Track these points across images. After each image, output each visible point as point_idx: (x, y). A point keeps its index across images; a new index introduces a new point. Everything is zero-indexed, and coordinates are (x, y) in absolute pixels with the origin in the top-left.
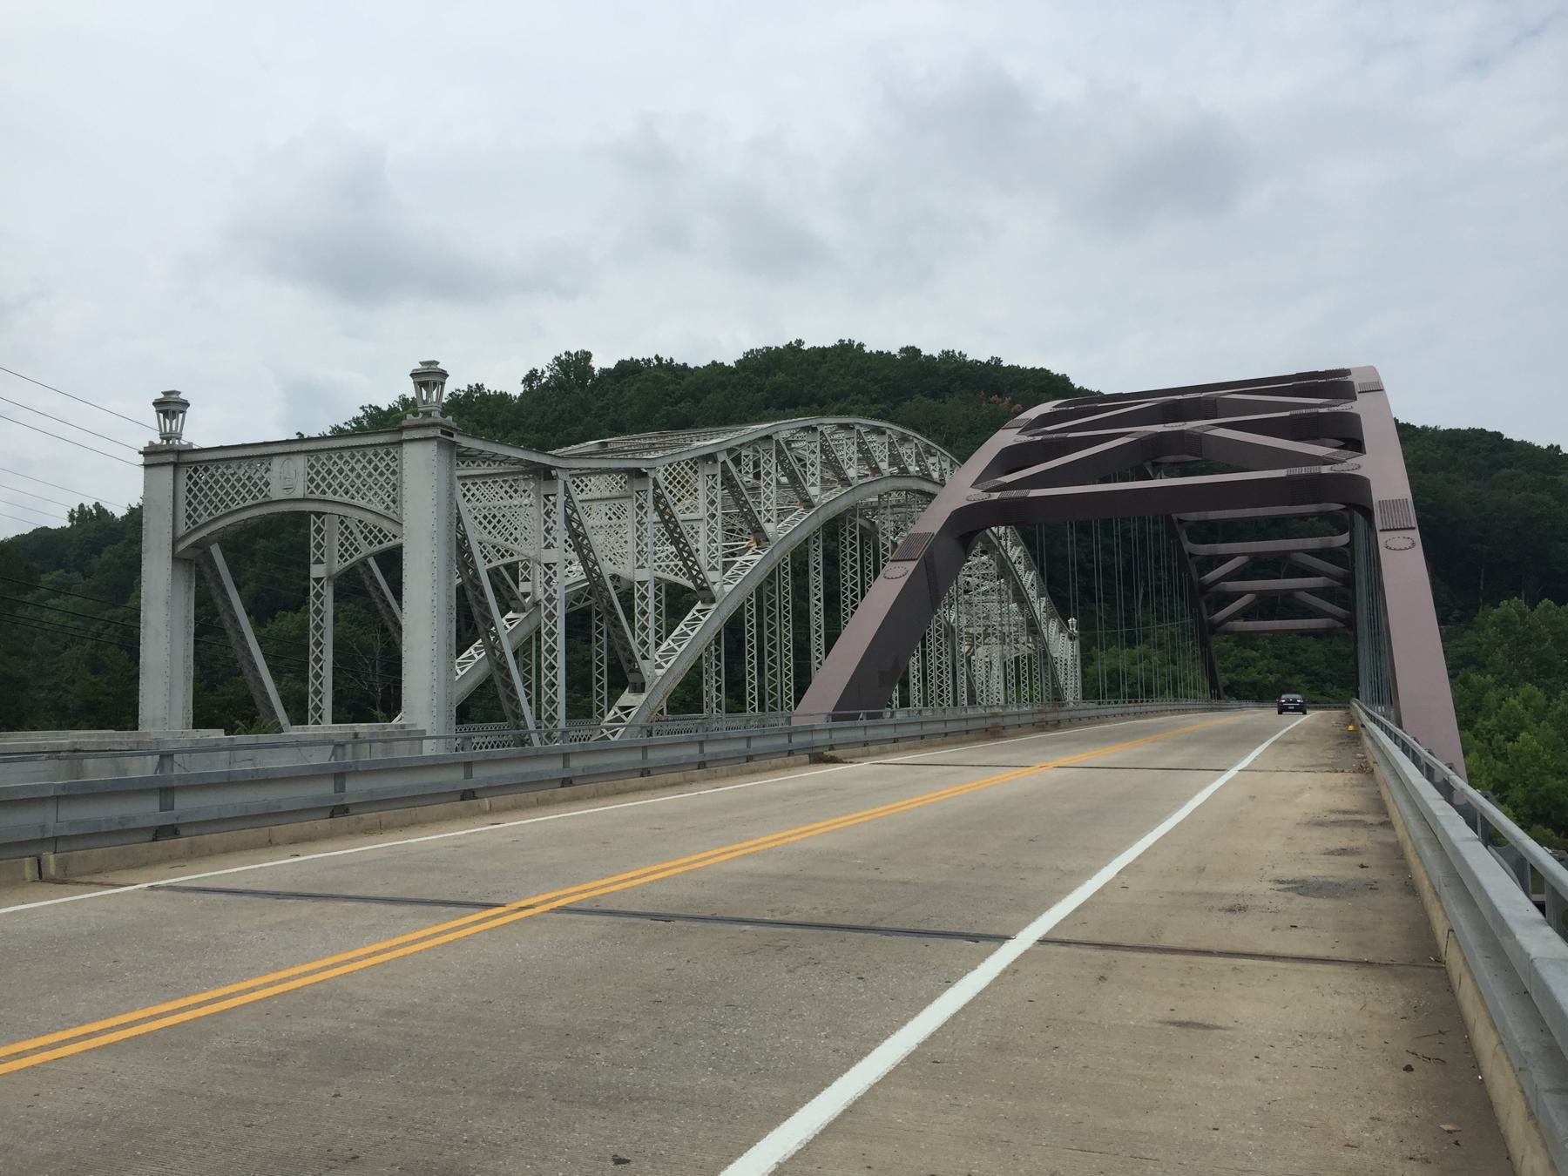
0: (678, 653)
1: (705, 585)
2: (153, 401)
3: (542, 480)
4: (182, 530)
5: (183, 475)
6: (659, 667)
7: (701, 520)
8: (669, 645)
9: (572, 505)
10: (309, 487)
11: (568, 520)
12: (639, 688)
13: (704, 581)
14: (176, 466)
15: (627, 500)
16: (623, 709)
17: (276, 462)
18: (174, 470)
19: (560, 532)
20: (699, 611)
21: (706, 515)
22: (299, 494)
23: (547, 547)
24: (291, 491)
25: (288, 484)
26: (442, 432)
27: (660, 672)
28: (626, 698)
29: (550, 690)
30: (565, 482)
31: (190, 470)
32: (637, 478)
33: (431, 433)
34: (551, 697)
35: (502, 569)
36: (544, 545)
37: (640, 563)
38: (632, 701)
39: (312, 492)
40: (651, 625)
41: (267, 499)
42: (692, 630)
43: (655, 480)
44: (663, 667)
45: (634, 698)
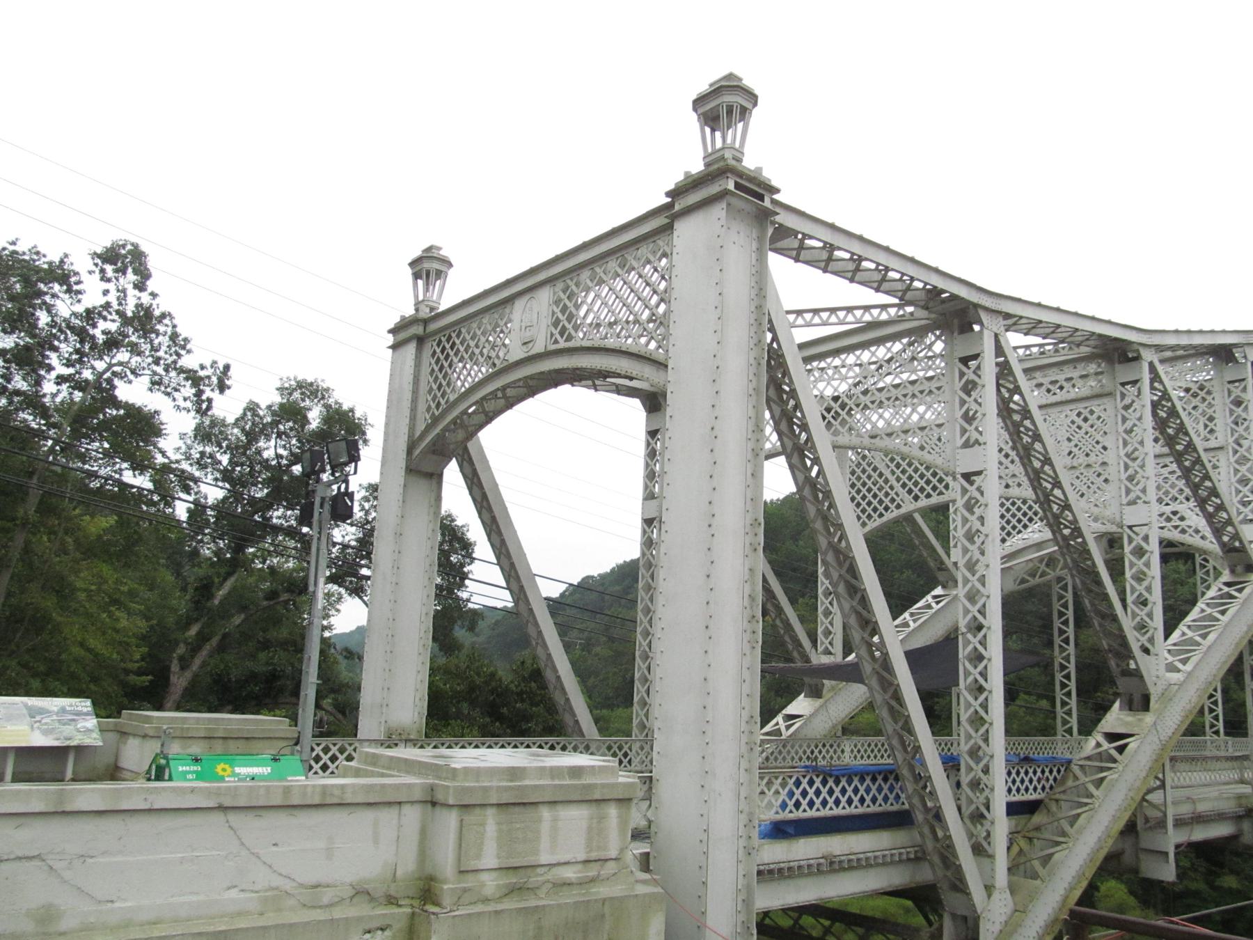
0: (1203, 648)
1: (1237, 544)
2: (410, 261)
3: (956, 334)
4: (421, 427)
5: (427, 352)
6: (1171, 668)
7: (1221, 448)
8: (1184, 634)
9: (1011, 379)
10: (552, 335)
11: (1004, 410)
12: (1140, 702)
13: (1236, 536)
14: (420, 340)
15: (1105, 400)
16: (1112, 737)
17: (519, 304)
18: (417, 349)
19: (992, 429)
20: (1228, 584)
21: (1231, 440)
22: (539, 348)
23: (967, 445)
24: (531, 345)
25: (527, 335)
26: (737, 186)
27: (1174, 677)
28: (1116, 718)
29: (976, 699)
30: (996, 335)
31: (435, 344)
32: (1120, 362)
33: (714, 189)
34: (976, 712)
35: (917, 517)
36: (960, 442)
37: (1132, 496)
38: (1127, 724)
39: (556, 342)
40: (1156, 597)
41: (505, 364)
42: (1223, 613)
43: (1151, 364)
44: (1179, 671)
45: (1130, 719)
